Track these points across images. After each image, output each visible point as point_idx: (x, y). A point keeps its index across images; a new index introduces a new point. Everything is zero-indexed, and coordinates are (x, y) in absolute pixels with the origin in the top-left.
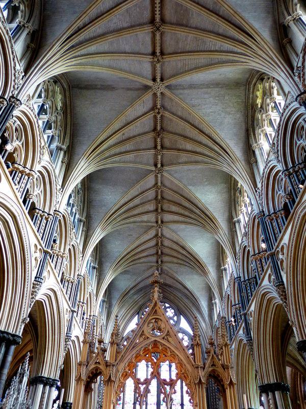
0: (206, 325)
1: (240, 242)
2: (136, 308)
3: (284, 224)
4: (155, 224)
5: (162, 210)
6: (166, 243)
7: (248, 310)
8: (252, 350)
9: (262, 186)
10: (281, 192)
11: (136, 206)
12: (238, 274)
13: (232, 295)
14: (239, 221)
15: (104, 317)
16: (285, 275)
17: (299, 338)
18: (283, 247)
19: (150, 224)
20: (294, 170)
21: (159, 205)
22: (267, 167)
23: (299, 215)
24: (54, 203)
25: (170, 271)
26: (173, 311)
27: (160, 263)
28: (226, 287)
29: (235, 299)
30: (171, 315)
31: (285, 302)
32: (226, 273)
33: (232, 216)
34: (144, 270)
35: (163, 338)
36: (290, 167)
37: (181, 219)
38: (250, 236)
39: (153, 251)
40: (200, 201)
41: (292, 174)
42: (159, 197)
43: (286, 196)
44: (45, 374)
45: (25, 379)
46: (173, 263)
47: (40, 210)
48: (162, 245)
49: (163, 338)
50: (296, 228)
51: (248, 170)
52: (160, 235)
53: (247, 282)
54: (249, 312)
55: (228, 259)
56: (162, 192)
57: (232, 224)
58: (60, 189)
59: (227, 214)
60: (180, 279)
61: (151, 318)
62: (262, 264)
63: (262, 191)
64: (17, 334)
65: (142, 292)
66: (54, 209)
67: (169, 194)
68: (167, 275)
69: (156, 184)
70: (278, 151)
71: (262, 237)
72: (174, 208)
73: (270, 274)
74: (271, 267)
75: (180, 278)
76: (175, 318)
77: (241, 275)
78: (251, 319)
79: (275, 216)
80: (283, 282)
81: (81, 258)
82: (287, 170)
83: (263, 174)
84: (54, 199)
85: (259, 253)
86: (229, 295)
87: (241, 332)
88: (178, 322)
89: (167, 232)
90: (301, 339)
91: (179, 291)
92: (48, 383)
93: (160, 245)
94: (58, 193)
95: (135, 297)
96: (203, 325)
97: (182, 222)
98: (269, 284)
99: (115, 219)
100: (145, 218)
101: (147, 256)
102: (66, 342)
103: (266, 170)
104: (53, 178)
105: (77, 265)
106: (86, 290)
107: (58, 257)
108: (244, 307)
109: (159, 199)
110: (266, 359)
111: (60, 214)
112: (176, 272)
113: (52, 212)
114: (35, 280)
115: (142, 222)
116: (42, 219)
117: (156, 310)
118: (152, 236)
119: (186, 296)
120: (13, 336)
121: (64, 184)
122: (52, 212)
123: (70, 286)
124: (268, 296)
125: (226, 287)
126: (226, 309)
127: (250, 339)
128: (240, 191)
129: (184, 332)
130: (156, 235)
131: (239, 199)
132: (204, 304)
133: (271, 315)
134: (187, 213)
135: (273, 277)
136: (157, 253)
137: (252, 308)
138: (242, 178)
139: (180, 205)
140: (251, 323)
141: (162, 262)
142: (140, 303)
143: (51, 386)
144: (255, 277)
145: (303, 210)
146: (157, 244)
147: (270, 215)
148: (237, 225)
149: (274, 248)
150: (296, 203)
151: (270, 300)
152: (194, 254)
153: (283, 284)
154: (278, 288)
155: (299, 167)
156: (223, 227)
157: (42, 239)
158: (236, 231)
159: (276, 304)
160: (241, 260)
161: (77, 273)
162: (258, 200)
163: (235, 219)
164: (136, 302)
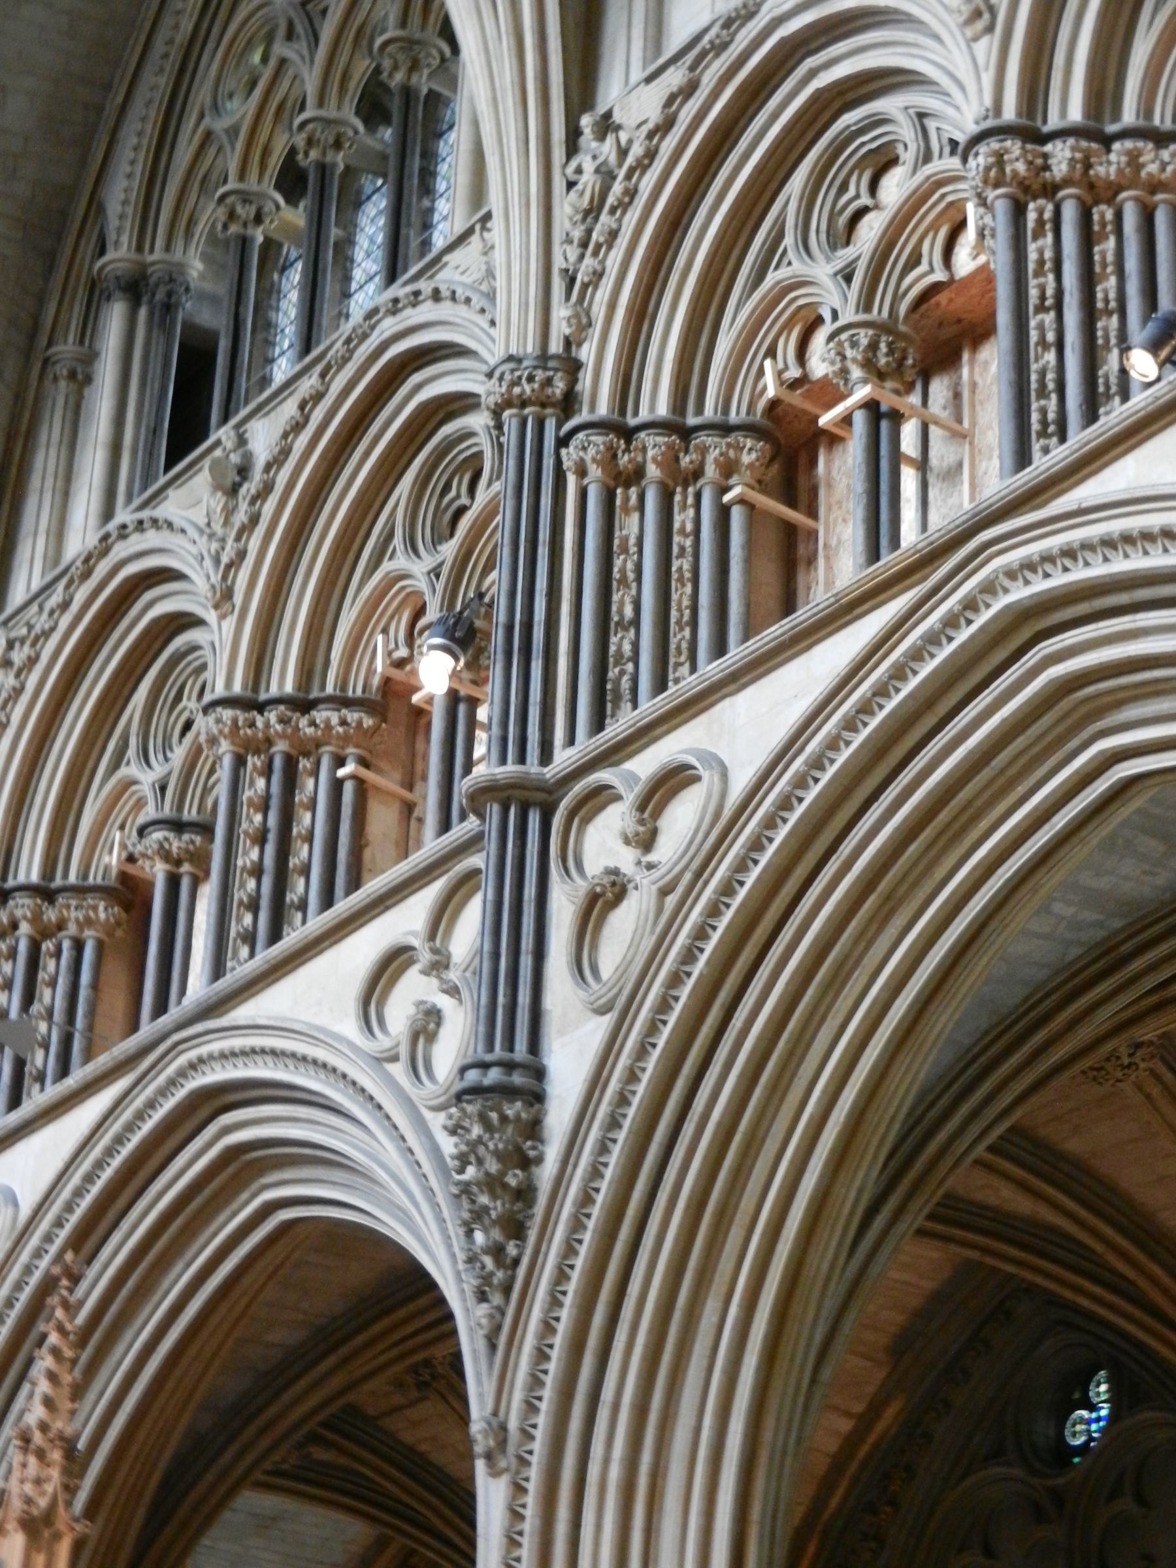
23: (990, 588)
41: (1050, 190)
43: (864, 337)
50: (899, 673)
79: (671, 461)
85: (303, 705)
98: (349, 1027)
145: (1047, 558)
147: (628, 434)
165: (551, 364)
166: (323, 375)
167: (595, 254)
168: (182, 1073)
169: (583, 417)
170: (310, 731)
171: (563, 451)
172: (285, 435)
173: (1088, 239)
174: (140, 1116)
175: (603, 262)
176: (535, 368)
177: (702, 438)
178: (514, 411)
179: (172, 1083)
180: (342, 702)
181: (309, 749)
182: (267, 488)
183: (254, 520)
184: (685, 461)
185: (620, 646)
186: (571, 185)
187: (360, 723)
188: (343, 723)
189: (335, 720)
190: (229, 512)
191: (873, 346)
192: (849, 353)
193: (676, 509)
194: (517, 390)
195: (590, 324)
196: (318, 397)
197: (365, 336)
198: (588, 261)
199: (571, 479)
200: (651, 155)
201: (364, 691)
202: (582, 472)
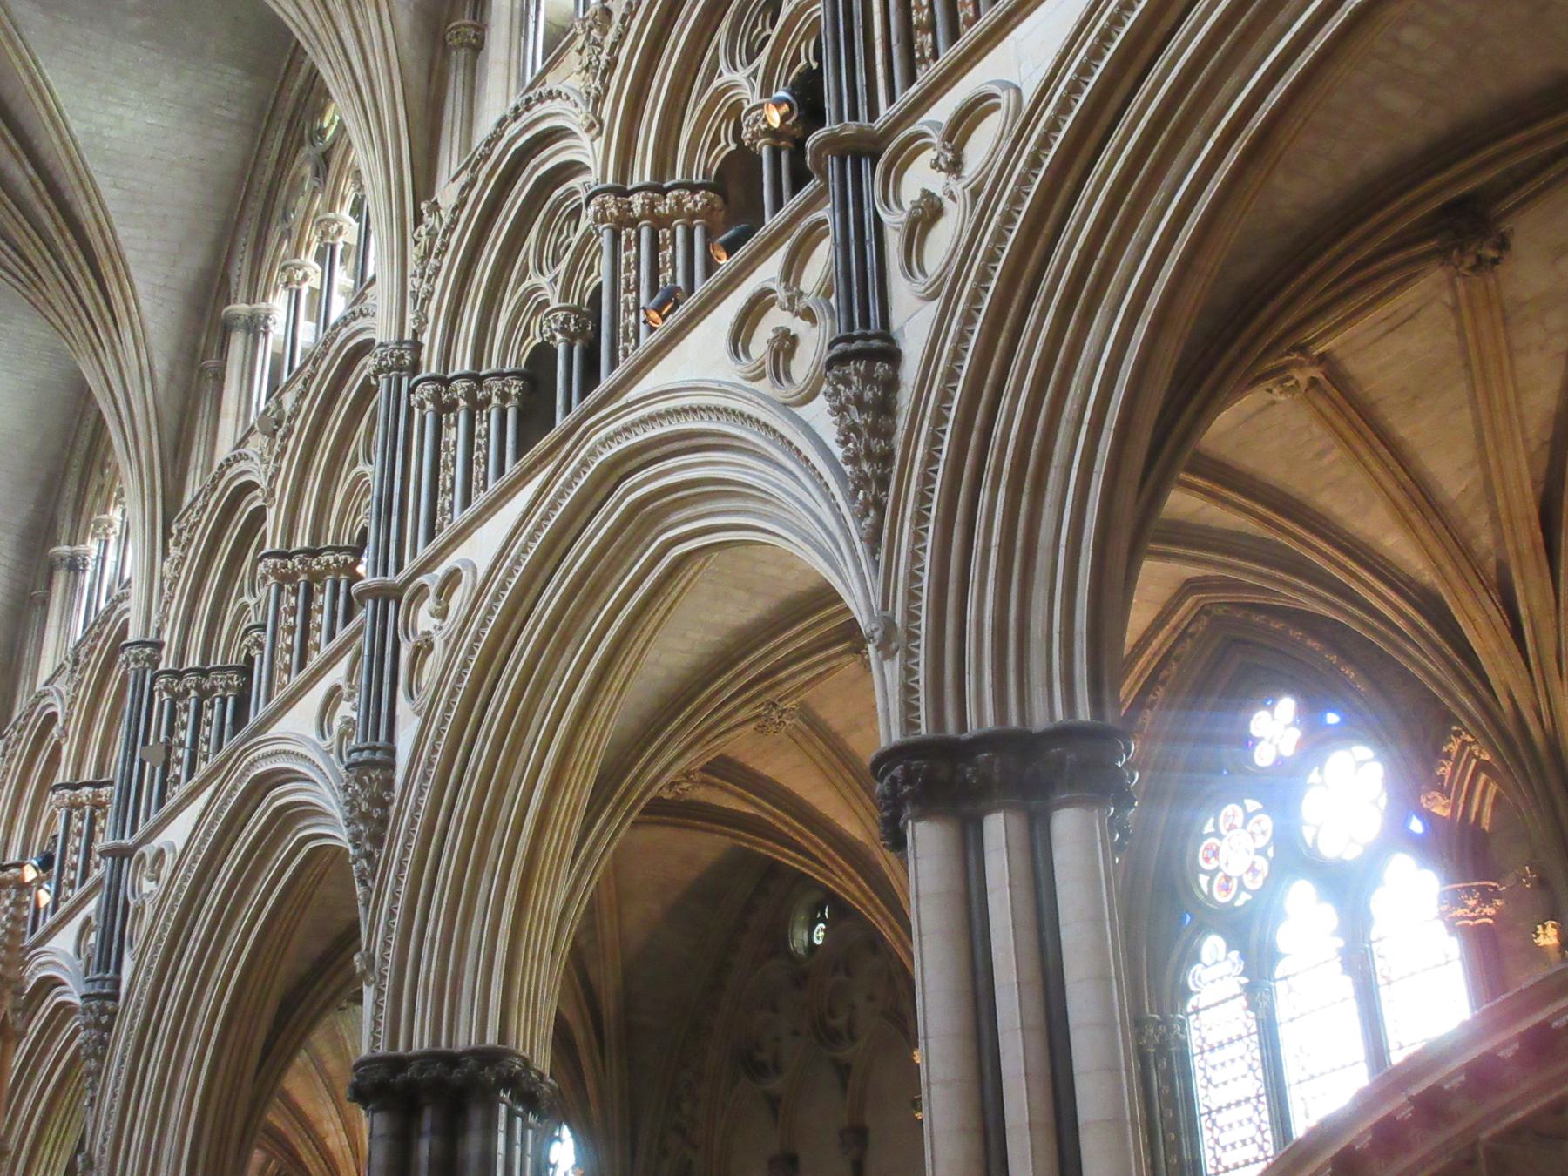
1: (224, 450)
8: (100, 1049)
9: (461, 204)
10: (546, 284)
12: (154, 625)
14: (256, 327)
16: (417, 722)
17: (376, 1039)
18: (453, 578)
20: (652, 206)
22: (526, 118)
23: (593, 453)
28: (46, 671)
31: (369, 856)
32: (72, 588)
33: (225, 280)
36: (636, 182)
41: (633, 223)
43: (561, 316)
50: (553, 506)
51: (418, 78)
53: (190, 680)
54: (149, 850)
55: (115, 514)
59: (195, 260)
63: (450, 229)
70: (612, 65)
73: (335, 691)
74: (359, 653)
78: (148, 887)
79: (470, 395)
80: (392, 752)
82: (621, 192)
83: (491, 141)
85: (314, 552)
86: (52, 717)
87: (65, 941)
103: (514, 128)
108: (126, 815)
110: (160, 1109)
124: (284, 795)
125: (46, 671)
127: (105, 997)
128: (326, 157)
131: (302, 202)
133: (265, 893)
135: (346, 710)
137: (177, 833)
138: (369, 108)
140: (140, 910)
144: (246, 670)
145: (618, 433)
147: (446, 382)
148: (237, 342)
151: (288, 817)
153: (391, 766)
154: (359, 780)
155: (679, 200)
156: (151, 326)
158: (220, 378)
159: (311, 845)
160: (195, 552)
162: (412, 266)
163: (240, 307)
165: (405, 346)
166: (314, 364)
167: (428, 282)
168: (247, 769)
169: (424, 374)
170: (318, 567)
171: (412, 395)
172: (297, 400)
173: (655, 248)
174: (229, 795)
175: (433, 287)
176: (394, 349)
177: (488, 381)
178: (384, 375)
179: (243, 774)
180: (337, 549)
181: (316, 577)
182: (290, 430)
183: (284, 449)
184: (480, 395)
185: (443, 504)
186: (416, 243)
187: (346, 560)
188: (336, 561)
189: (331, 561)
190: (271, 446)
191: (566, 320)
192: (553, 326)
193: (477, 423)
194: (384, 363)
195: (427, 322)
196: (312, 377)
197: (334, 340)
198: (425, 286)
199: (417, 411)
200: (455, 222)
201: (349, 543)
202: (422, 405)
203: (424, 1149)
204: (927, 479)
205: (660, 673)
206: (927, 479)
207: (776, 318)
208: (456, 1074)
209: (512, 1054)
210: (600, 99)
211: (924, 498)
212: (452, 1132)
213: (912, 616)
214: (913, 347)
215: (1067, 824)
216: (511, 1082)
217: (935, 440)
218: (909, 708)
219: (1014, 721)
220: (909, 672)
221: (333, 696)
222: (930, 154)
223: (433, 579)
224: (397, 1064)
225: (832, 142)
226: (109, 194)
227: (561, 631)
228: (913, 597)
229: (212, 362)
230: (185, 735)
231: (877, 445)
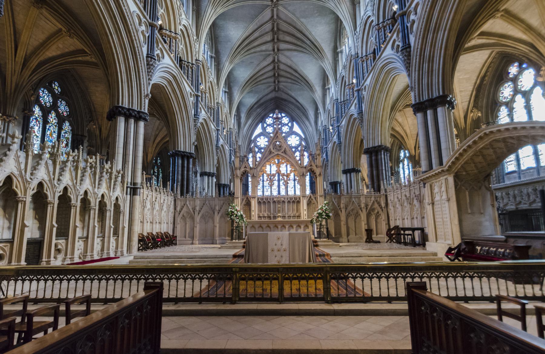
0: (313, 129)
2: (259, 118)
3: (371, 66)
4: (272, 52)
5: (278, 39)
6: (282, 67)
7: (341, 124)
8: (340, 150)
11: (256, 39)
13: (332, 111)
14: (341, 52)
15: (236, 127)
19: (268, 53)
21: (276, 36)
22: (366, 15)
24: (194, 53)
25: (285, 89)
26: (288, 119)
27: (277, 83)
29: (334, 114)
30: (287, 122)
32: (329, 92)
34: (264, 89)
35: (282, 152)
37: (294, 47)
38: (348, 69)
39: (271, 74)
40: (310, 33)
42: (275, 29)
44: (207, 170)
45: (198, 175)
46: (287, 82)
47: (185, 61)
48: (278, 68)
49: (282, 152)
51: (352, 12)
52: (276, 60)
53: (342, 103)
54: (341, 125)
56: (278, 24)
57: (336, 53)
58: (196, 39)
59: (332, 45)
60: (293, 94)
61: (274, 141)
62: (353, 92)
64: (192, 152)
65: (264, 106)
66: (195, 58)
67: (284, 26)
68: (283, 91)
69: (273, 16)
71: (355, 75)
72: (288, 38)
75: (293, 94)
76: (290, 124)
77: (339, 98)
79: (366, 58)
80: (362, 111)
81: (217, 90)
84: (193, 49)
87: (335, 137)
88: (291, 128)
89: (283, 59)
90: (367, 147)
91: (292, 103)
92: (209, 175)
93: (276, 68)
94: (195, 44)
95: (258, 110)
96: (310, 129)
97: (295, 50)
99: (239, 52)
100: (264, 48)
101: (266, 78)
102: (217, 150)
104: (190, 32)
105: (215, 95)
106: (223, 111)
107: (202, 94)
108: (338, 121)
109: (276, 31)
111: (201, 63)
112: (290, 90)
113: (194, 62)
114: (194, 117)
115: (262, 51)
116: (188, 68)
117: (277, 137)
118: (270, 62)
119: (299, 108)
120: (190, 153)
121: (198, 34)
122: (194, 62)
123: (212, 112)
126: (327, 120)
127: (340, 143)
129: (297, 134)
130: (274, 61)
132: (311, 114)
134: (299, 43)
136: (275, 75)
137: (343, 123)
139: (293, 36)
141: (278, 82)
142: (263, 115)
143: (212, 176)
146: (274, 68)
147: (362, 58)
148: (340, 55)
149: (361, 85)
150: (376, 59)
152: (304, 77)
153: (362, 112)
155: (387, 23)
157: (192, 85)
161: (216, 102)
164: (259, 114)
173: (384, 31)
203: (373, 158)
204: (416, 65)
205: (398, 91)
206: (416, 65)
207: (397, 43)
208: (376, 149)
209: (382, 146)
210: (373, 10)
211: (415, 68)
212: (377, 156)
213: (415, 85)
214: (412, 45)
215: (439, 110)
216: (383, 149)
217: (416, 59)
218: (415, 98)
219: (430, 97)
220: (415, 93)
221: (356, 104)
222: (412, 13)
223: (363, 87)
224: (368, 149)
225: (399, 15)
226: (319, 40)
227: (380, 91)
228: (415, 83)
229: (337, 59)
230: (343, 110)
231: (408, 61)
